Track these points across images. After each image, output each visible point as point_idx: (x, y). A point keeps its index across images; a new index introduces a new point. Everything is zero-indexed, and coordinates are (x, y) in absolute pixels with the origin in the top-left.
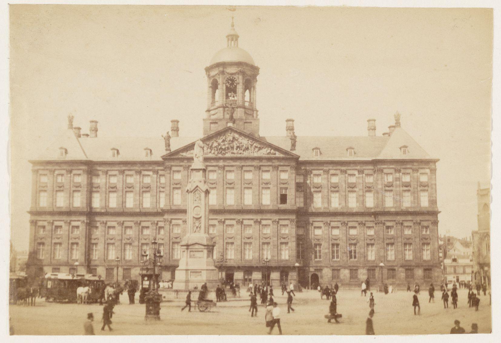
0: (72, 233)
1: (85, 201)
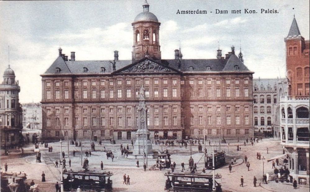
0: (65, 112)
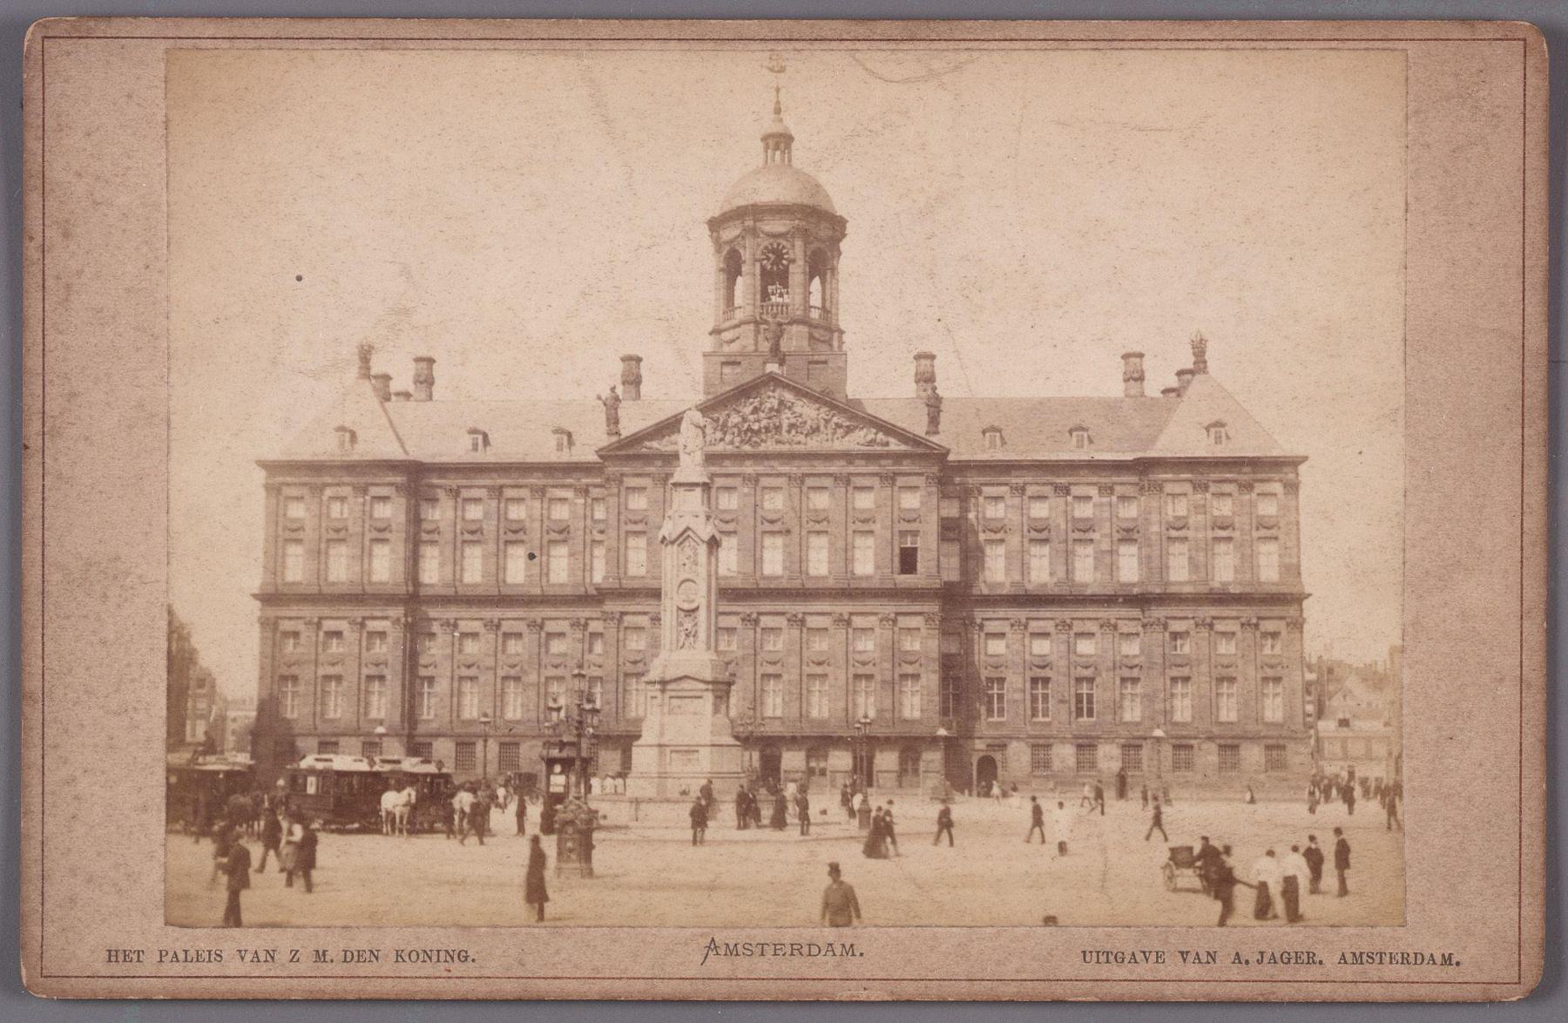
0: (368, 649)
1: (401, 568)
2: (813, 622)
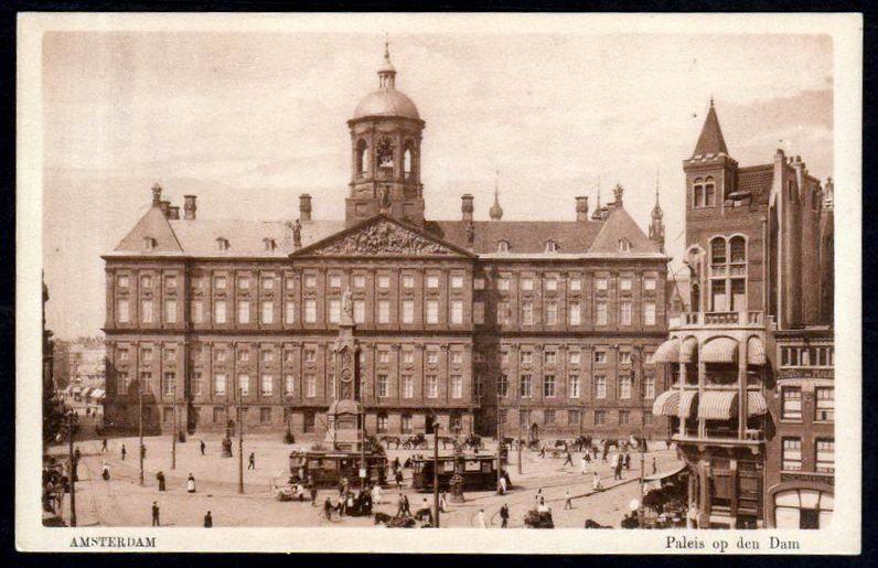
2: (404, 347)
